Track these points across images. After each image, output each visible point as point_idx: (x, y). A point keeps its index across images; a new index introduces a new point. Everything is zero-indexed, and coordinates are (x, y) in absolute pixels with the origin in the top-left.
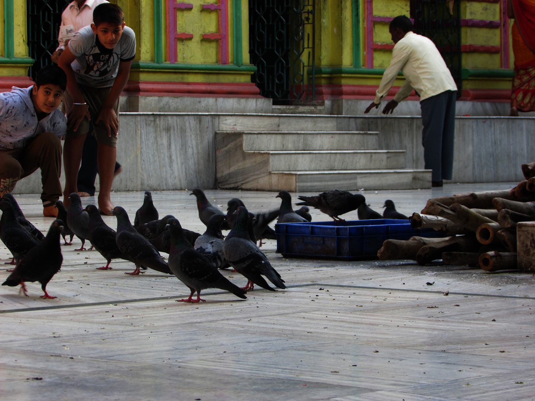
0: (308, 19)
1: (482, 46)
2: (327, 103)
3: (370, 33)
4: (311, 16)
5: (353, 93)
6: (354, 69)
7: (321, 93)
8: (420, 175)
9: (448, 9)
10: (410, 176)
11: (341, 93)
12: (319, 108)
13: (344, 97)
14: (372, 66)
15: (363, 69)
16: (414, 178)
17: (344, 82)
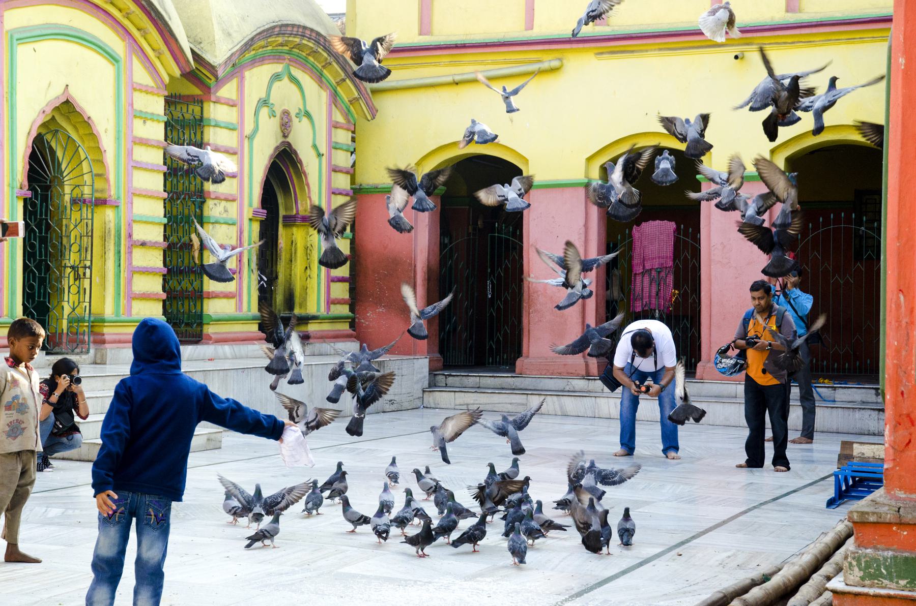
0: (84, 274)
1: (222, 292)
2: (92, 351)
3: (129, 282)
4: (88, 271)
5: (114, 342)
6: (115, 318)
7: (83, 342)
8: (213, 436)
9: (193, 258)
10: (205, 438)
11: (103, 342)
12: (84, 357)
13: (107, 345)
14: (131, 315)
15: (123, 318)
16: (208, 440)
17: (105, 330)
